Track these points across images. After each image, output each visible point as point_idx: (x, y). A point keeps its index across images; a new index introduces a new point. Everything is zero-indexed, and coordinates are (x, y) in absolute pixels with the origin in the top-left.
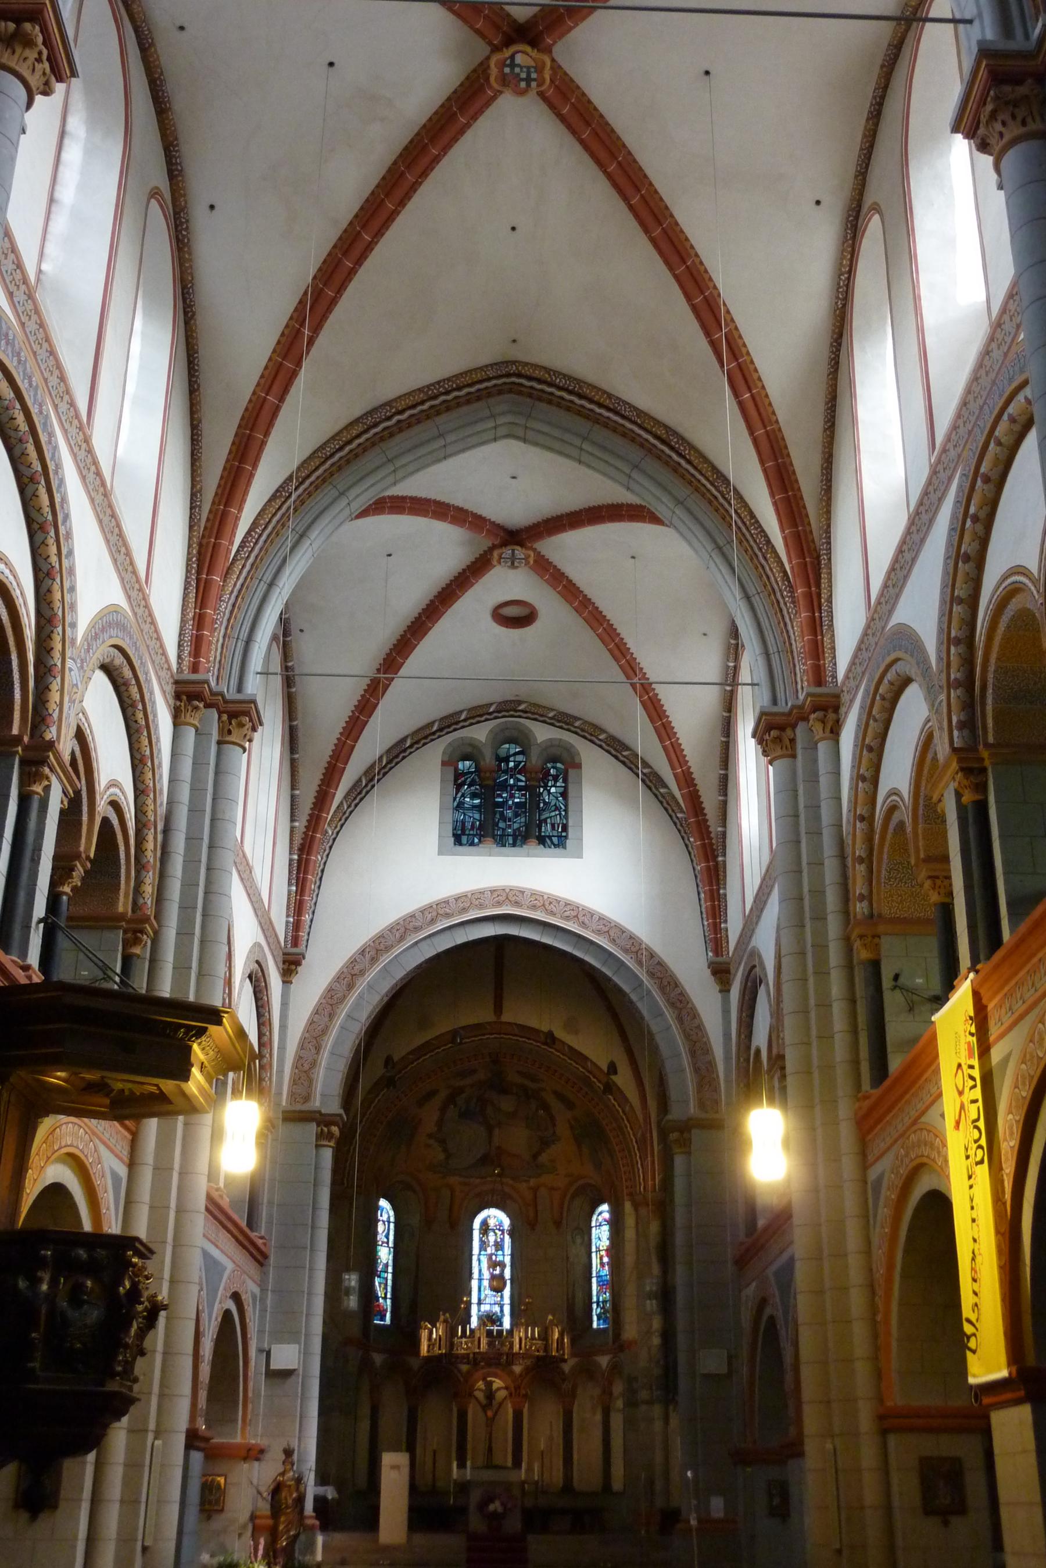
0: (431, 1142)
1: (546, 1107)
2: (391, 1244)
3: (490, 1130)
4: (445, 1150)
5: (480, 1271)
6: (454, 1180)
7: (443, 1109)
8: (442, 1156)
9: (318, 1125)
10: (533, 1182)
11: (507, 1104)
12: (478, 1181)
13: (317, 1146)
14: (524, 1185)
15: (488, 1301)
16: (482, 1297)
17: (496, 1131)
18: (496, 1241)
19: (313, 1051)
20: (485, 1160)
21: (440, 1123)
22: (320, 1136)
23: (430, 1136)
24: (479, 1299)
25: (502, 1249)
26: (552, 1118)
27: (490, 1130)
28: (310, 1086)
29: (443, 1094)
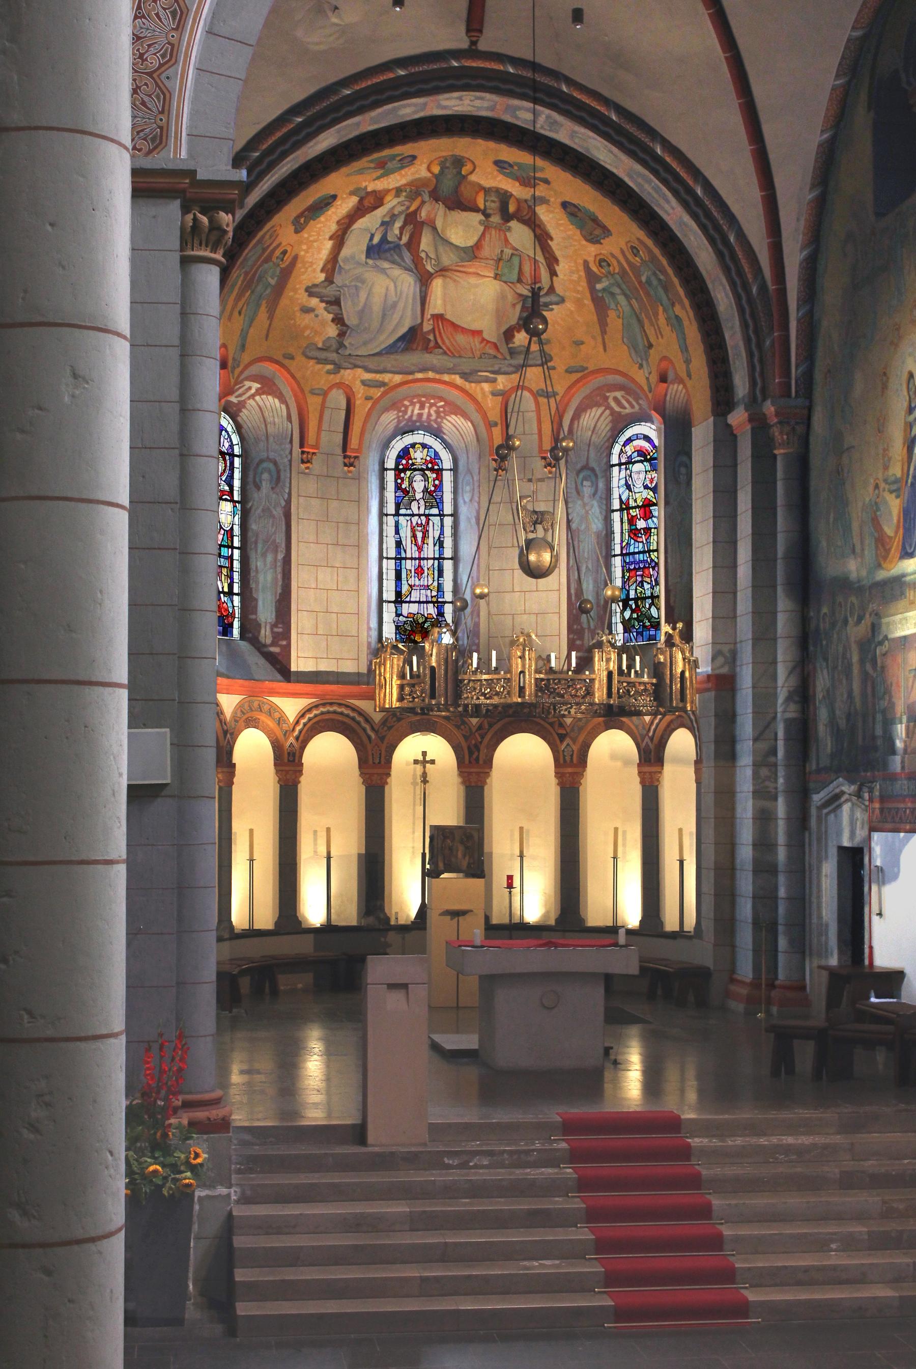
0: (314, 302)
1: (542, 238)
2: (236, 497)
3: (425, 280)
4: (338, 320)
5: (399, 544)
6: (354, 377)
7: (339, 239)
8: (332, 331)
9: (185, 209)
10: (503, 382)
11: (461, 230)
12: (398, 378)
13: (186, 261)
14: (486, 386)
15: (415, 596)
16: (405, 588)
17: (437, 284)
18: (425, 490)
19: (169, 22)
20: (412, 339)
21: (332, 265)
22: (190, 235)
23: (311, 291)
24: (398, 594)
25: (439, 504)
26: (552, 261)
27: (425, 280)
28: (165, 110)
29: (345, 206)
